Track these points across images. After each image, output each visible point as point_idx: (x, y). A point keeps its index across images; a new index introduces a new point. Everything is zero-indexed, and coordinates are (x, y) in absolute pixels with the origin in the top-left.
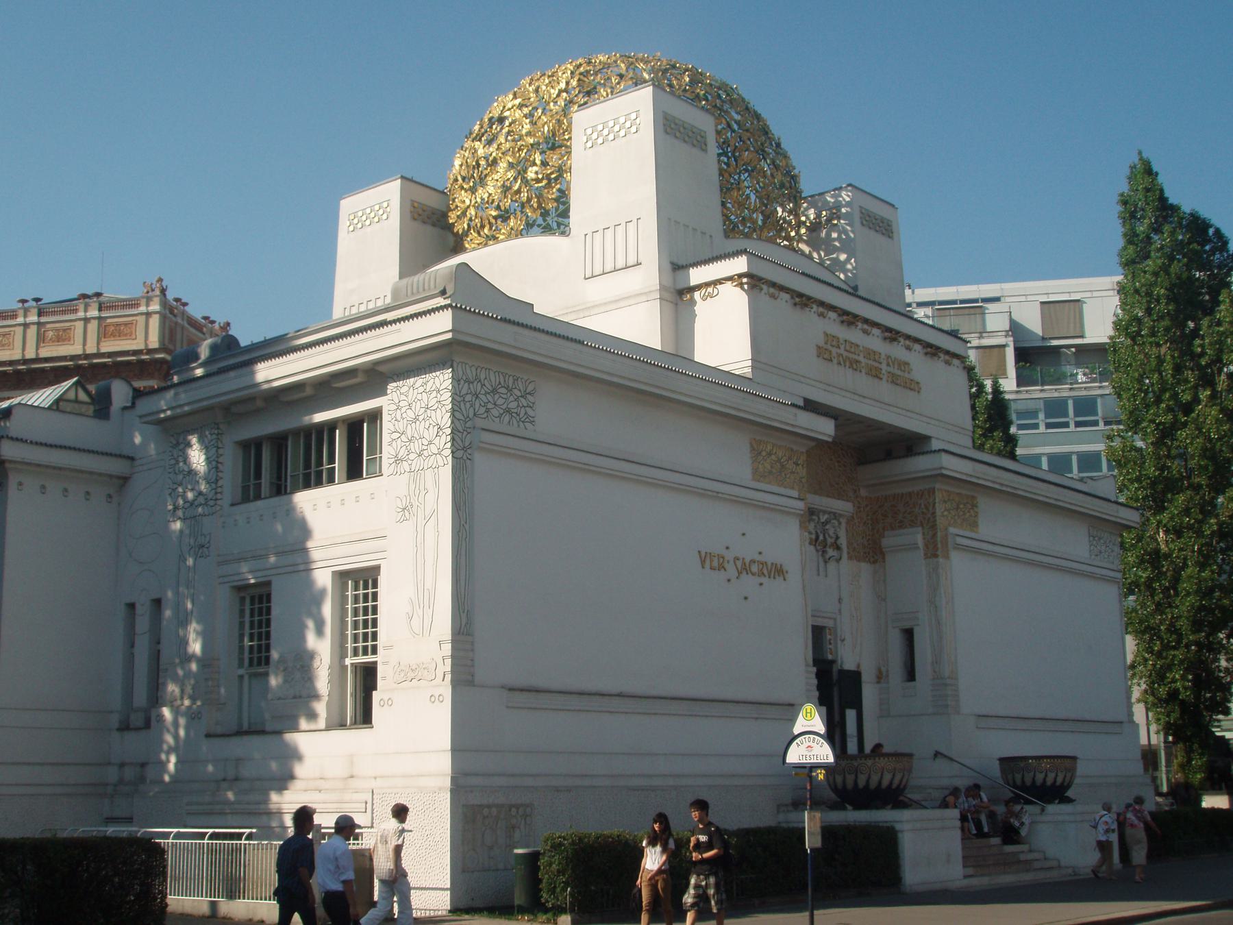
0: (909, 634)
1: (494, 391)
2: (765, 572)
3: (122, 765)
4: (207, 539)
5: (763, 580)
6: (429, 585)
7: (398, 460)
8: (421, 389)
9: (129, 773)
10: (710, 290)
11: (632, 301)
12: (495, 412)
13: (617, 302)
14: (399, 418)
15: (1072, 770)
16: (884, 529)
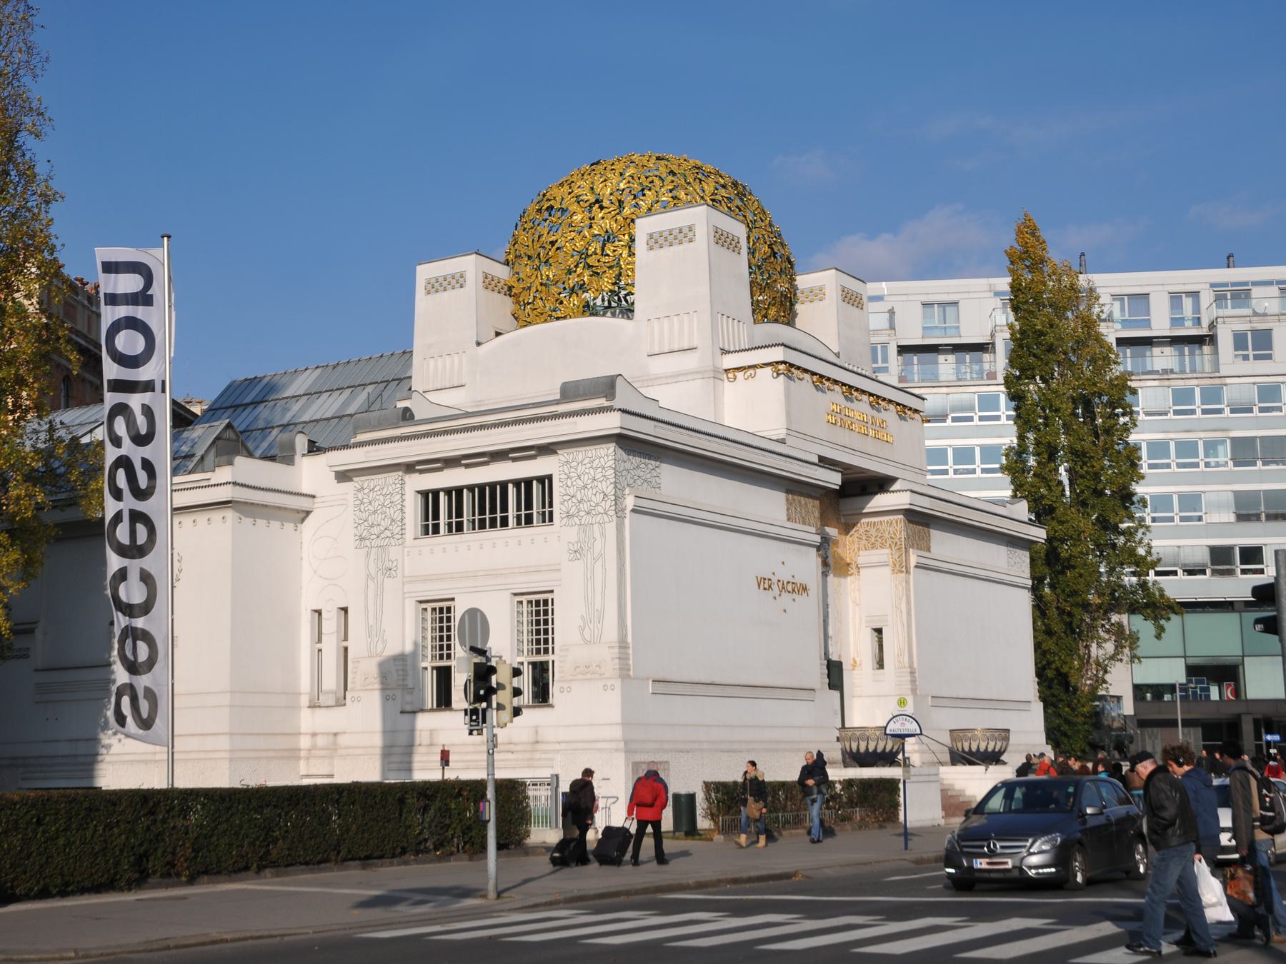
0: (879, 631)
1: (638, 467)
2: (796, 590)
3: (314, 735)
4: (395, 563)
5: (795, 596)
6: (598, 606)
7: (569, 516)
8: (589, 465)
9: (321, 741)
10: (752, 371)
11: (689, 377)
12: (639, 482)
13: (675, 377)
14: (569, 485)
15: (1007, 739)
16: (859, 549)
